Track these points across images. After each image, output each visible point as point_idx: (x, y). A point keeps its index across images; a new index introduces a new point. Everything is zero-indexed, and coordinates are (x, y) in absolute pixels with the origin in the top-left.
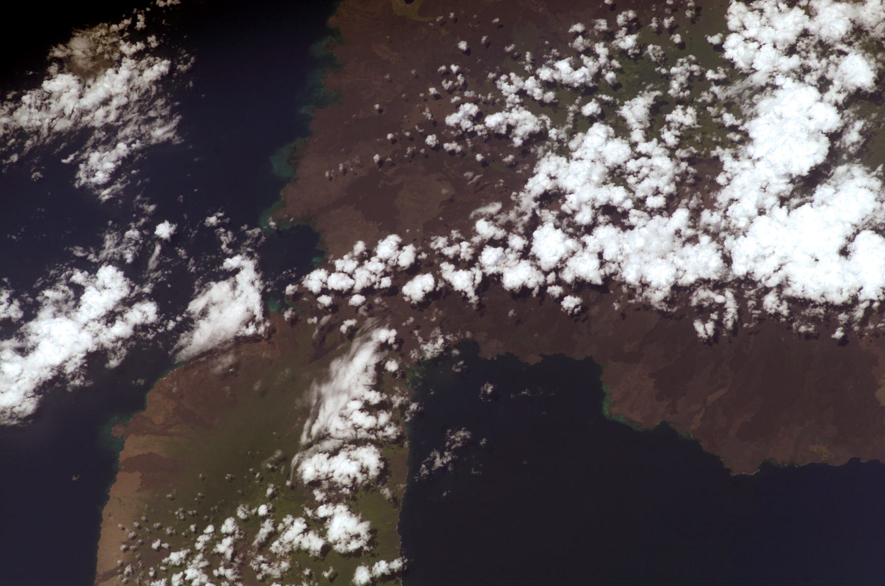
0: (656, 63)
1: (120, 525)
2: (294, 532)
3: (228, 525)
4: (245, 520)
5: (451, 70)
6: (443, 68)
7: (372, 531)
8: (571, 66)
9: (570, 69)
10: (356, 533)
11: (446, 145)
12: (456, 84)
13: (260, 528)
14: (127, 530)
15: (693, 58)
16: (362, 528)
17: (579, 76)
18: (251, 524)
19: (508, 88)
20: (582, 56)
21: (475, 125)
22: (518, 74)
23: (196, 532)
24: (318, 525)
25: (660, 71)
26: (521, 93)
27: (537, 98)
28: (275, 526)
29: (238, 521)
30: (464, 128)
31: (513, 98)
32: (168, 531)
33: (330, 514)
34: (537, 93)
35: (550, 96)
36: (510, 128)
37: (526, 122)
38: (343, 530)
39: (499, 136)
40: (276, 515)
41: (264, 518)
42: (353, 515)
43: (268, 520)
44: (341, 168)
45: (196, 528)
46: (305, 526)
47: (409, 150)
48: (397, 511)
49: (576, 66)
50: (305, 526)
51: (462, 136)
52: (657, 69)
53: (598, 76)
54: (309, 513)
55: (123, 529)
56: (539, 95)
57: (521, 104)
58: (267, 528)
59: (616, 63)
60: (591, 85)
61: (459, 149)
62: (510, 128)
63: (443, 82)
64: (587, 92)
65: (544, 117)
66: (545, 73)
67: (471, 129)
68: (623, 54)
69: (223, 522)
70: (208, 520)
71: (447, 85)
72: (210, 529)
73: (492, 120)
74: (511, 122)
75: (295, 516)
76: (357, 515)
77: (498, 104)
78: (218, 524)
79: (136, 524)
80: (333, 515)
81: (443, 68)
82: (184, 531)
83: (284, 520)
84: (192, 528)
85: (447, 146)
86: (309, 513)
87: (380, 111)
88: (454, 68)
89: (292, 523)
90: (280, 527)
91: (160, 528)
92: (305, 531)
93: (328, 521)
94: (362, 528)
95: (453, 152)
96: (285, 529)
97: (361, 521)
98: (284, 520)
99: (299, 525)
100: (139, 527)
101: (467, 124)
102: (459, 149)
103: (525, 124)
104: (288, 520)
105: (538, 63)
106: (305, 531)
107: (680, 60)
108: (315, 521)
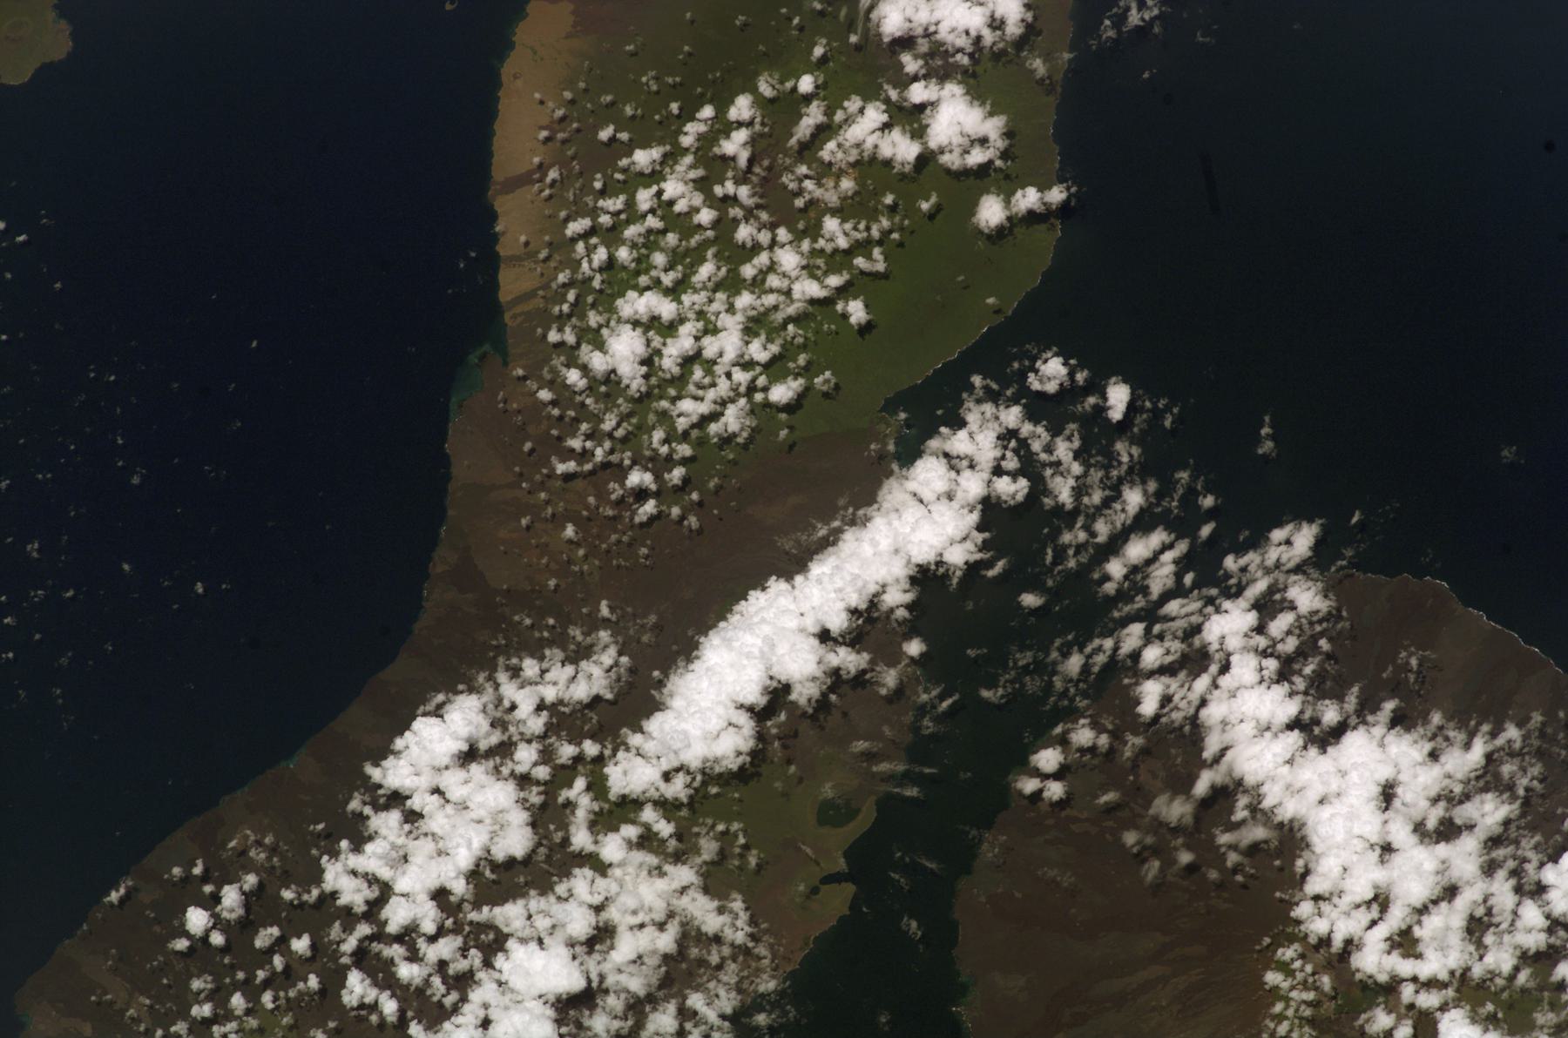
1: (537, 96)
2: (865, 126)
3: (742, 107)
4: (772, 101)
7: (1008, 134)
10: (980, 134)
13: (800, 116)
14: (551, 104)
16: (993, 128)
18: (785, 107)
23: (679, 117)
24: (912, 118)
28: (829, 112)
29: (760, 102)
32: (629, 111)
33: (933, 98)
38: (957, 129)
40: (831, 95)
41: (807, 99)
42: (976, 103)
43: (815, 103)
45: (680, 109)
46: (884, 118)
48: (1052, 101)
50: (884, 118)
54: (893, 94)
55: (542, 102)
58: (813, 116)
69: (731, 101)
70: (702, 95)
72: (707, 112)
75: (867, 98)
76: (983, 104)
78: (722, 105)
79: (568, 95)
80: (938, 100)
82: (659, 113)
83: (846, 104)
84: (674, 107)
86: (893, 94)
89: (862, 111)
90: (839, 116)
91: (613, 104)
92: (886, 127)
93: (928, 111)
94: (993, 128)
96: (849, 121)
97: (991, 114)
98: (846, 104)
99: (874, 115)
100: (572, 102)
104: (853, 104)
106: (886, 127)
108: (900, 109)
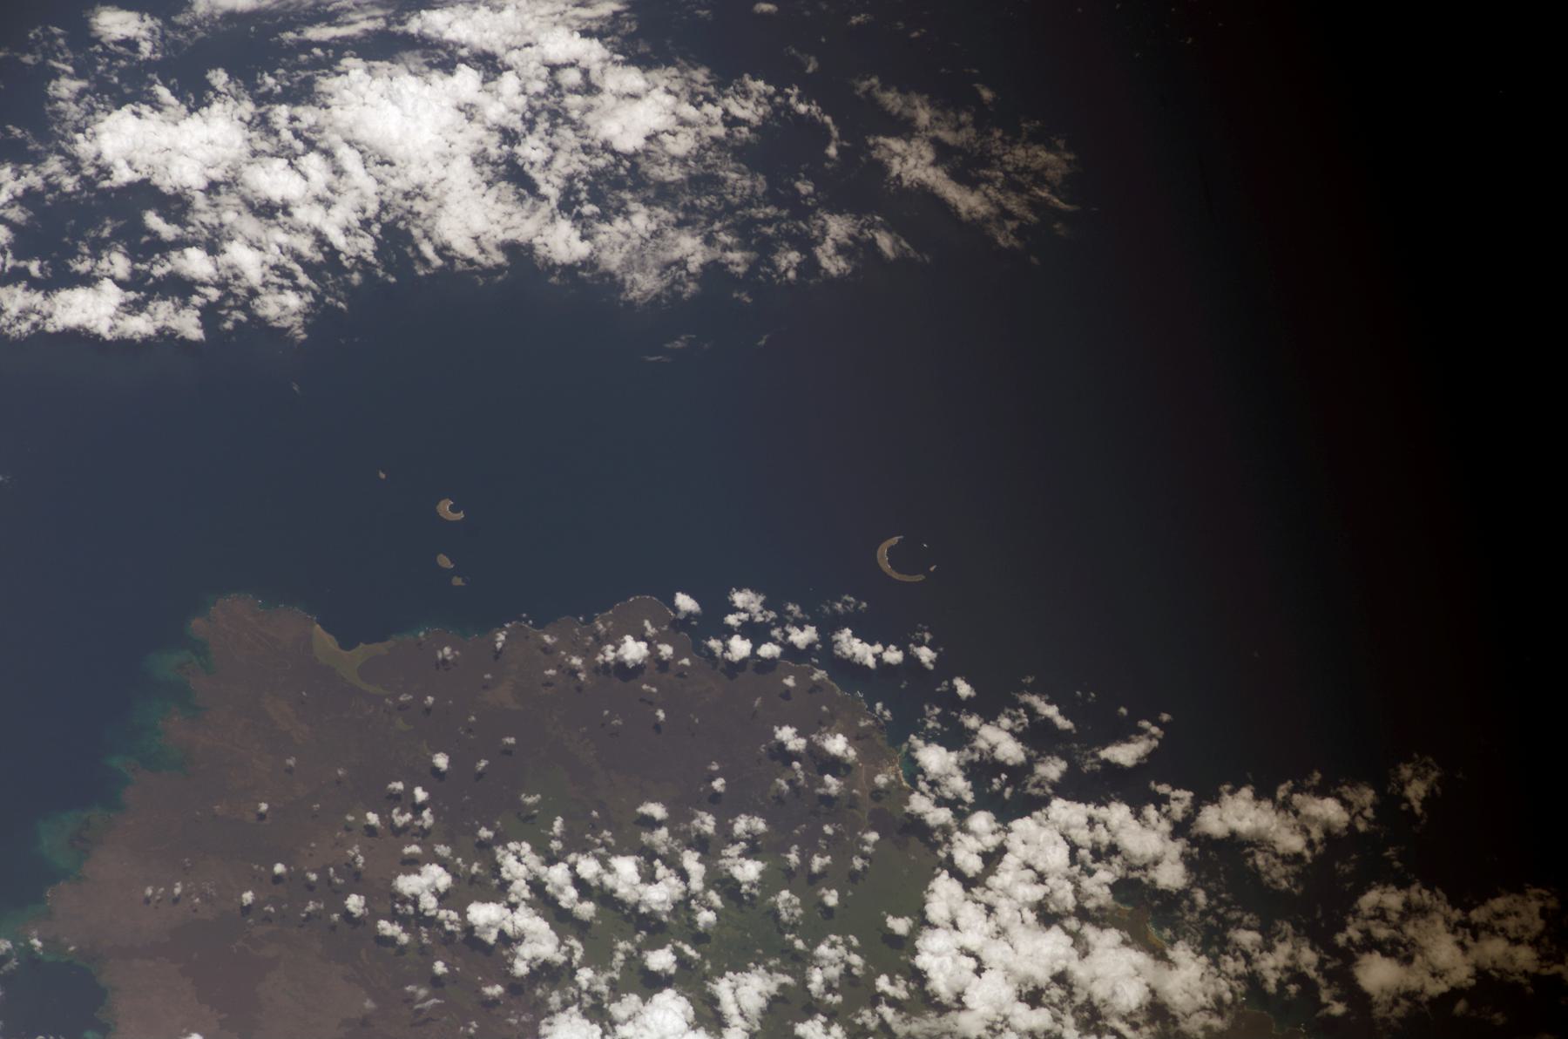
0: (786, 925)
5: (413, 796)
6: (399, 786)
8: (639, 873)
9: (637, 879)
11: (383, 924)
12: (418, 823)
15: (855, 942)
17: (660, 895)
19: (518, 863)
20: (657, 862)
21: (440, 907)
22: (536, 850)
25: (791, 942)
26: (537, 885)
27: (564, 904)
30: (421, 906)
31: (520, 889)
34: (569, 896)
35: (587, 909)
36: (519, 939)
37: (540, 942)
39: (480, 945)
44: (178, 891)
47: (311, 906)
49: (649, 877)
51: (416, 920)
52: (788, 937)
53: (683, 906)
56: (571, 901)
57: (530, 904)
59: (715, 898)
60: (665, 918)
61: (404, 938)
62: (519, 939)
63: (396, 811)
64: (653, 928)
65: (575, 943)
66: (588, 867)
67: (433, 913)
68: (727, 886)
71: (402, 819)
73: (483, 914)
74: (509, 929)
77: (498, 891)
81: (399, 786)
85: (387, 928)
87: (262, 816)
88: (420, 795)
95: (392, 940)
101: (429, 903)
102: (404, 938)
103: (540, 943)
105: (577, 843)
107: (833, 937)
